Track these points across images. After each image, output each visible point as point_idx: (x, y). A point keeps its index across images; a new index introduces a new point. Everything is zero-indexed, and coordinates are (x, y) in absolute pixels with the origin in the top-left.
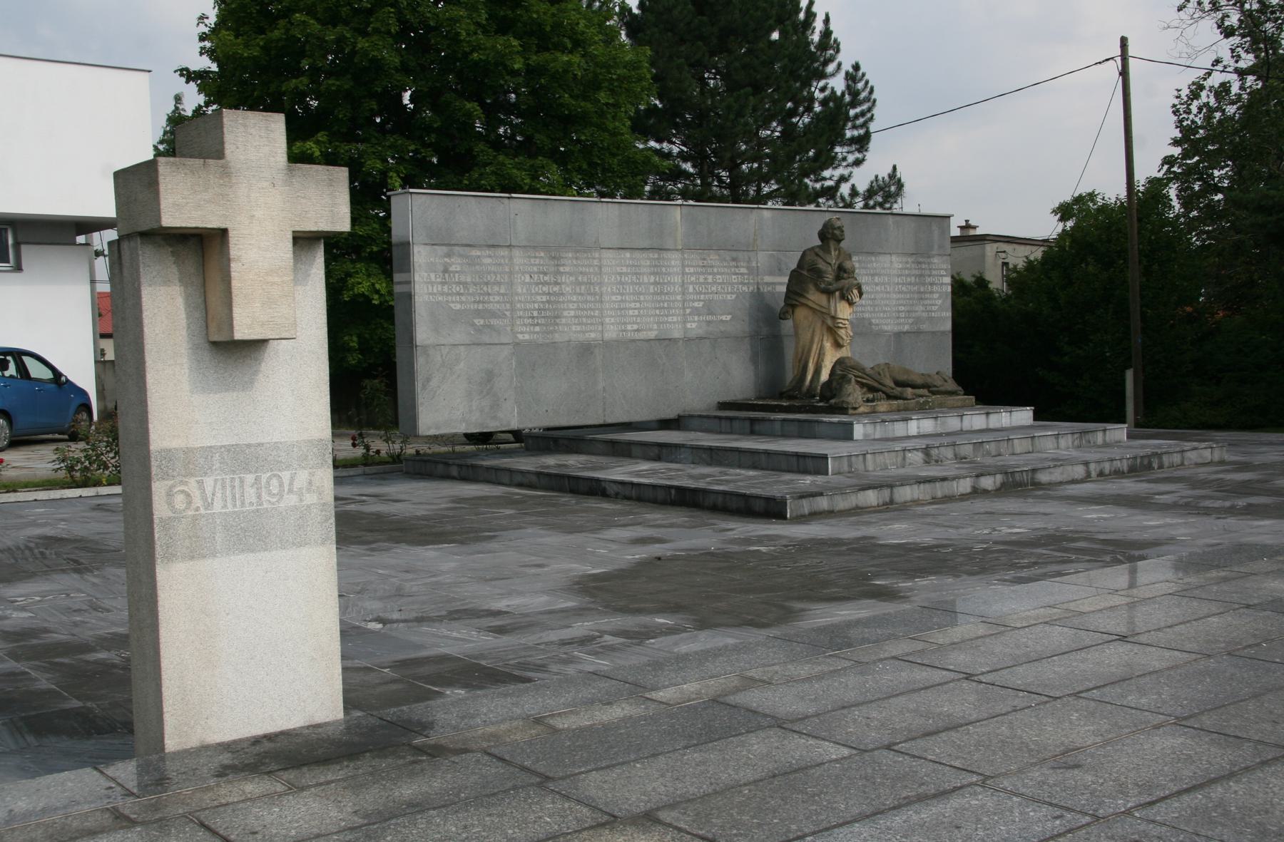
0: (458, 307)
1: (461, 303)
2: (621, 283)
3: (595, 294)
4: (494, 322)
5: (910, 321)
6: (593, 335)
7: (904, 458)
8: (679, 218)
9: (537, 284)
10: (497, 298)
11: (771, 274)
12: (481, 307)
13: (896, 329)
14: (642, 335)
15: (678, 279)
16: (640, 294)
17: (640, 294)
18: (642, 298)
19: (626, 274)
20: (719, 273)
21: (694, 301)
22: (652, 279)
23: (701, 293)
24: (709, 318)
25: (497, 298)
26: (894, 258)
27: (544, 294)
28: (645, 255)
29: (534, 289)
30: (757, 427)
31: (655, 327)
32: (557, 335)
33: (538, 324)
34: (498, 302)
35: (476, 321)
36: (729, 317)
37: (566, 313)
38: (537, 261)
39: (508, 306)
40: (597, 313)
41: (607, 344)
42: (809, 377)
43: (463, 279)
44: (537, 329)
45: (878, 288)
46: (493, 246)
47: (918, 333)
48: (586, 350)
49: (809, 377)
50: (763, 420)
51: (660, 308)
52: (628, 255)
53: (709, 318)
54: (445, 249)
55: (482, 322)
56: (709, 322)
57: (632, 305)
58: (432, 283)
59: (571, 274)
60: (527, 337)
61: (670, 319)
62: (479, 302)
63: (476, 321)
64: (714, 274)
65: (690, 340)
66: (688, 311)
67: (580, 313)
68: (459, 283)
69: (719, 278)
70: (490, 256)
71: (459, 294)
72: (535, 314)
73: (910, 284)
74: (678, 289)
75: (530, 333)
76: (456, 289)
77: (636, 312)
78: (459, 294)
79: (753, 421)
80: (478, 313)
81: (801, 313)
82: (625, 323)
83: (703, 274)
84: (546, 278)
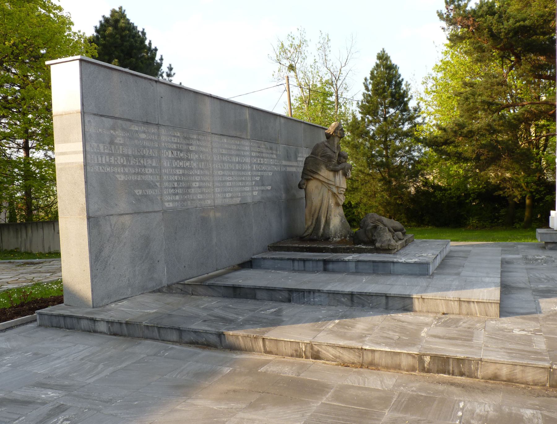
1: (125, 174)
2: (223, 162)
4: (150, 192)
9: (176, 159)
11: (285, 160)
17: (232, 170)
19: (225, 155)
24: (263, 188)
25: (151, 170)
27: (180, 168)
29: (175, 164)
30: (330, 266)
34: (151, 174)
35: (136, 191)
42: (322, 226)
44: (177, 198)
49: (322, 226)
50: (338, 261)
51: (242, 181)
53: (263, 188)
56: (263, 191)
58: (102, 154)
60: (171, 205)
62: (138, 174)
63: (136, 191)
67: (202, 184)
68: (123, 155)
71: (124, 166)
78: (124, 166)
79: (326, 262)
80: (138, 184)
81: (312, 185)
84: (182, 155)
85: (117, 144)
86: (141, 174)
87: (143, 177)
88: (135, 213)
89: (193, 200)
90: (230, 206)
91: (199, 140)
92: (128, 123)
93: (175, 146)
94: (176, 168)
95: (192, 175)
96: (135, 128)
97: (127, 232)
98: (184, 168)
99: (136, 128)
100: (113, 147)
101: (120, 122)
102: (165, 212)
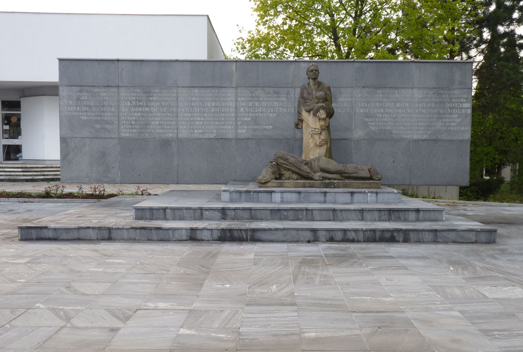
0: (85, 118)
1: (87, 116)
3: (173, 112)
4: (107, 126)
5: (429, 132)
6: (171, 135)
7: (202, 214)
8: (234, 69)
9: (135, 107)
10: (109, 114)
12: (99, 118)
13: (415, 137)
14: (206, 136)
15: (232, 104)
16: (205, 112)
17: (205, 112)
18: (206, 115)
19: (195, 101)
20: (263, 101)
21: (244, 117)
22: (214, 104)
23: (249, 112)
25: (109, 114)
26: (415, 91)
27: (139, 112)
28: (208, 90)
31: (215, 131)
32: (147, 135)
33: (135, 128)
34: (110, 116)
35: (96, 126)
36: (271, 127)
37: (153, 123)
38: (135, 94)
39: (116, 118)
40: (174, 123)
41: (179, 141)
43: (88, 103)
44: (134, 131)
45: (400, 111)
46: (108, 86)
47: (436, 141)
48: (166, 143)
51: (219, 121)
52: (197, 90)
54: (78, 88)
55: (100, 126)
56: (255, 130)
57: (199, 119)
58: (70, 106)
59: (157, 101)
60: (127, 135)
61: (226, 127)
62: (98, 116)
63: (96, 126)
64: (259, 101)
65: (240, 139)
66: (239, 123)
69: (264, 104)
70: (105, 92)
71: (86, 111)
72: (133, 122)
73: (430, 108)
74: (232, 110)
75: (129, 133)
76: (84, 109)
77: (201, 123)
78: (86, 111)
82: (193, 129)
83: (251, 101)
84: (140, 104)
85: (82, 100)
86: (101, 116)
87: (102, 118)
88: (94, 138)
89: (151, 133)
90: (200, 139)
91: (161, 93)
92: (92, 88)
93: (134, 99)
94: (135, 112)
95: (152, 117)
96: (96, 90)
97: (87, 148)
98: (142, 112)
99: (98, 90)
100: (79, 102)
101: (85, 88)
102: (120, 139)
